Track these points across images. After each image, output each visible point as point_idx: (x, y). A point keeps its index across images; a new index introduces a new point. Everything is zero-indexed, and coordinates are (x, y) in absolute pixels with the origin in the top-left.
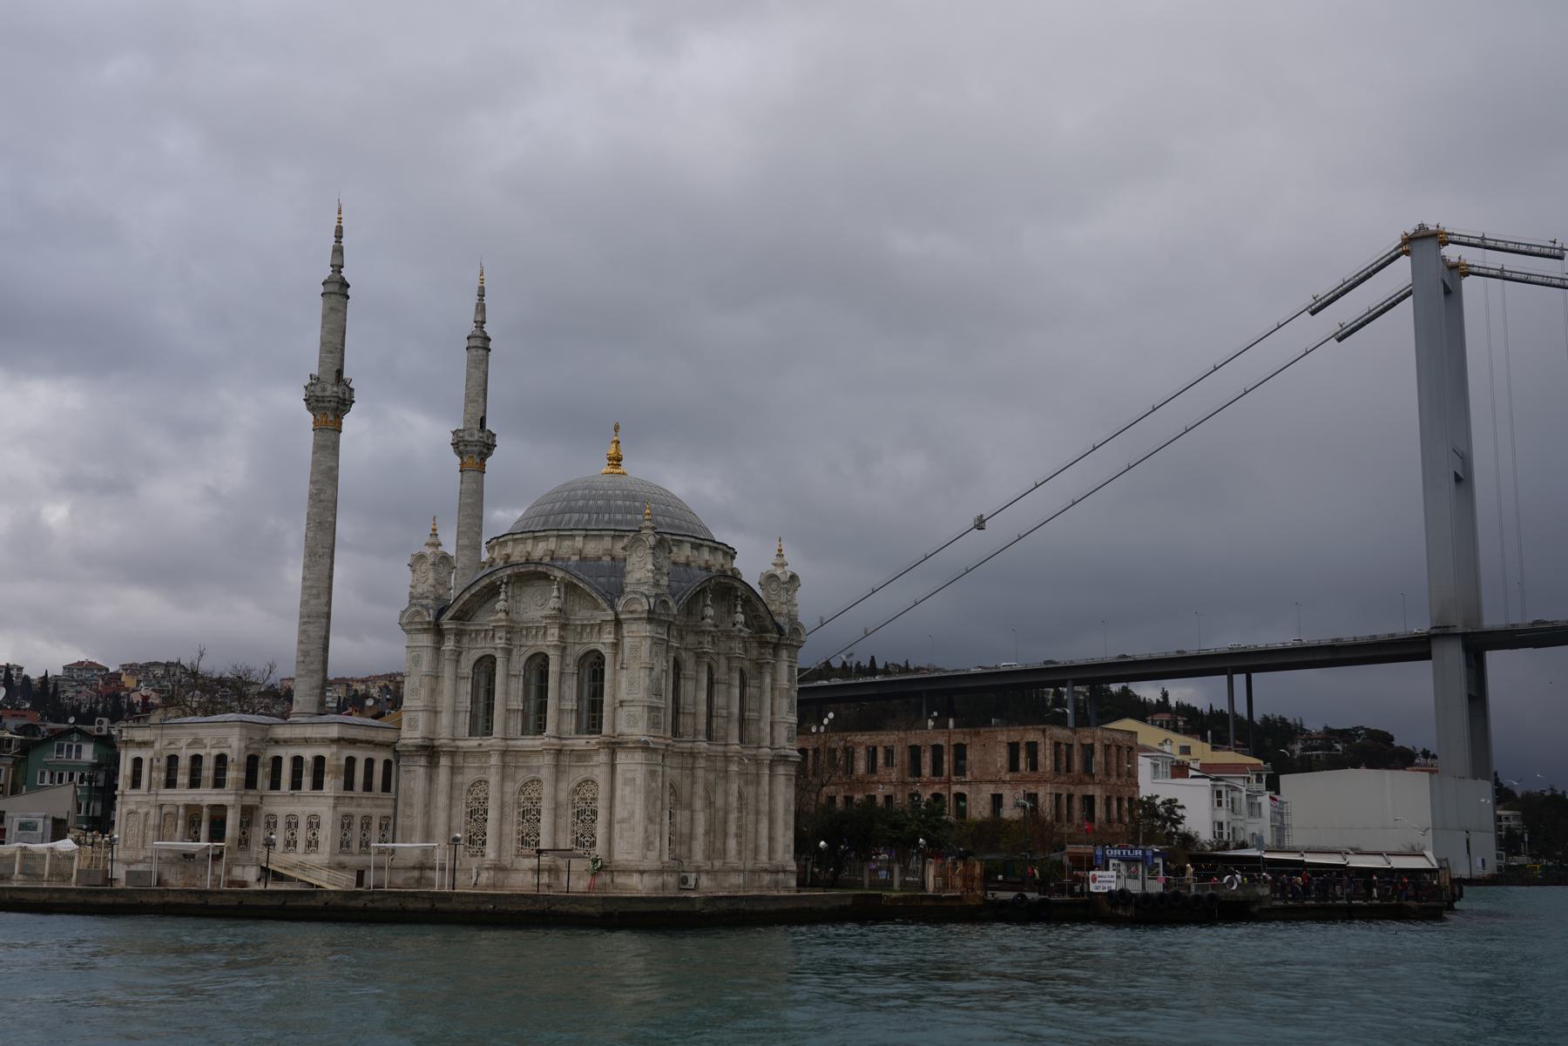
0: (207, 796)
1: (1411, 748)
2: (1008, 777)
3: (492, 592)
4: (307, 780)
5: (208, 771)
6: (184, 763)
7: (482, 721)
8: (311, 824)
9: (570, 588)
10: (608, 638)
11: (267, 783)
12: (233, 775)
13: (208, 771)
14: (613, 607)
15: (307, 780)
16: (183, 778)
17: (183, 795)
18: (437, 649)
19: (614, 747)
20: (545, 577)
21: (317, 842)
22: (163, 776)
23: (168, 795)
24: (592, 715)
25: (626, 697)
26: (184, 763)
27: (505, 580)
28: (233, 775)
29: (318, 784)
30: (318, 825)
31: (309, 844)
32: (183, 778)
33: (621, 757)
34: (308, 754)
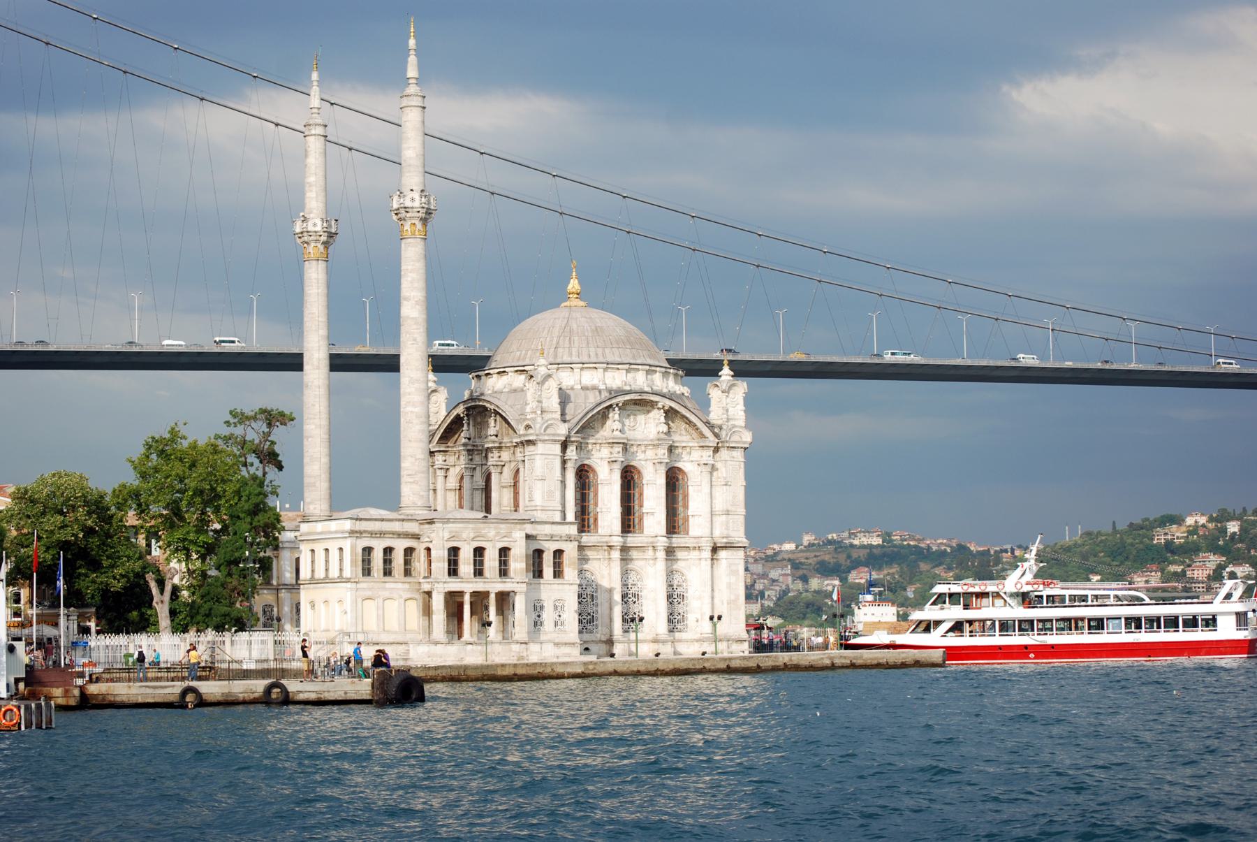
0: (492, 584)
3: (603, 415)
5: (491, 561)
6: (466, 556)
8: (556, 607)
9: (670, 414)
11: (471, 569)
12: (518, 564)
13: (491, 561)
15: (548, 570)
16: (466, 567)
17: (467, 584)
20: (652, 404)
21: (562, 624)
25: (730, 508)
27: (620, 405)
28: (518, 564)
29: (558, 573)
30: (562, 607)
31: (556, 624)
32: (466, 567)
33: (722, 554)
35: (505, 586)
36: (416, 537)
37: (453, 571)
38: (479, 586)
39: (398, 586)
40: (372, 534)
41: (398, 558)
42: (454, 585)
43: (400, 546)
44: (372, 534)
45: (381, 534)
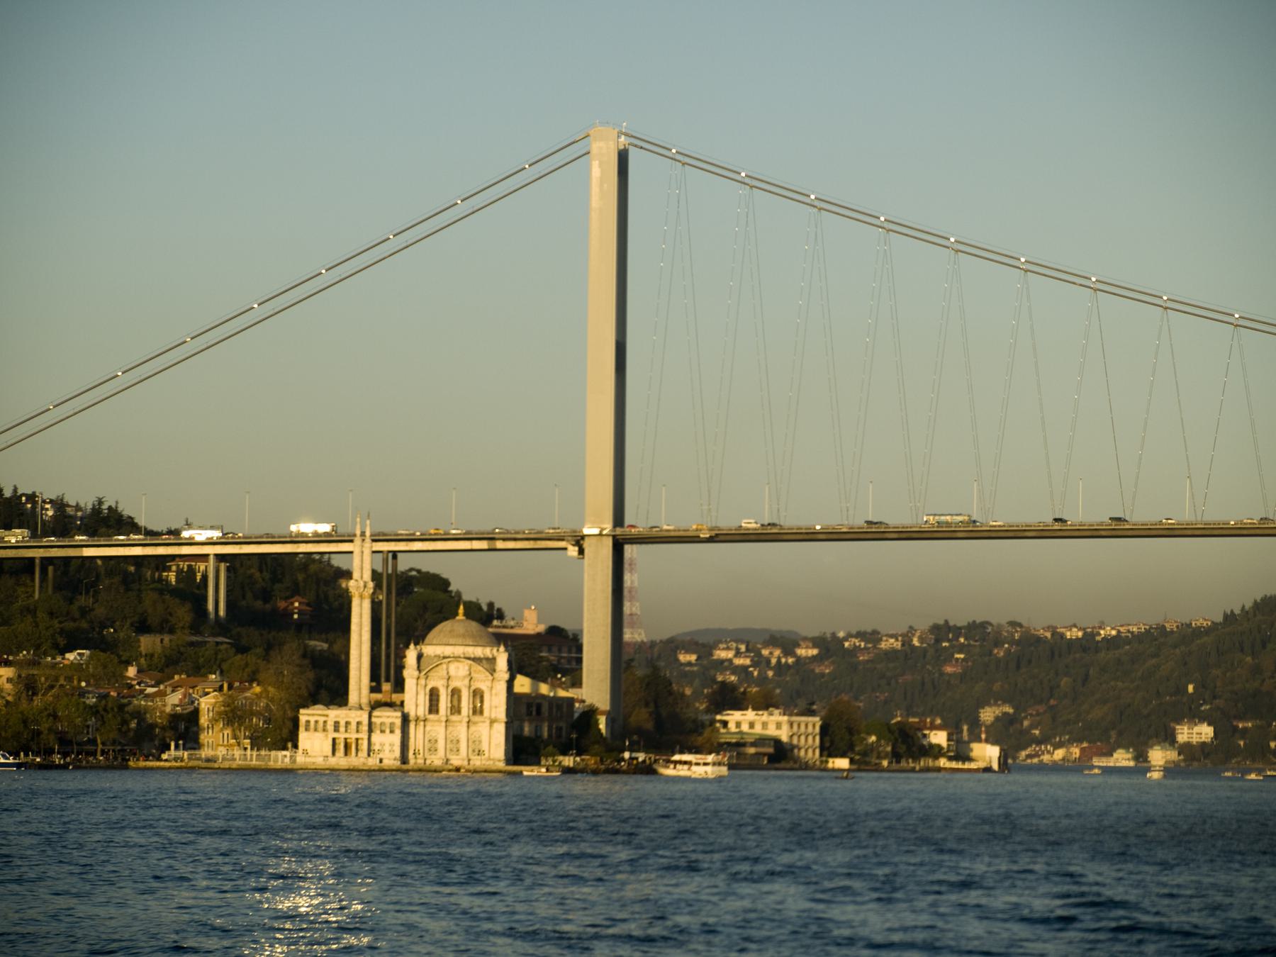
0: (352, 736)
1: (474, 600)
2: (527, 718)
4: (388, 731)
6: (342, 723)
7: (433, 707)
10: (489, 684)
13: (353, 726)
14: (492, 675)
18: (417, 684)
19: (492, 722)
22: (333, 728)
23: (336, 735)
24: (477, 711)
26: (342, 723)
28: (365, 728)
29: (392, 732)
32: (342, 729)
33: (495, 725)
34: (388, 721)
35: (359, 736)
36: (327, 716)
37: (336, 729)
38: (347, 735)
39: (320, 735)
40: (309, 715)
41: (321, 725)
42: (336, 735)
43: (321, 719)
44: (309, 715)
45: (313, 715)
